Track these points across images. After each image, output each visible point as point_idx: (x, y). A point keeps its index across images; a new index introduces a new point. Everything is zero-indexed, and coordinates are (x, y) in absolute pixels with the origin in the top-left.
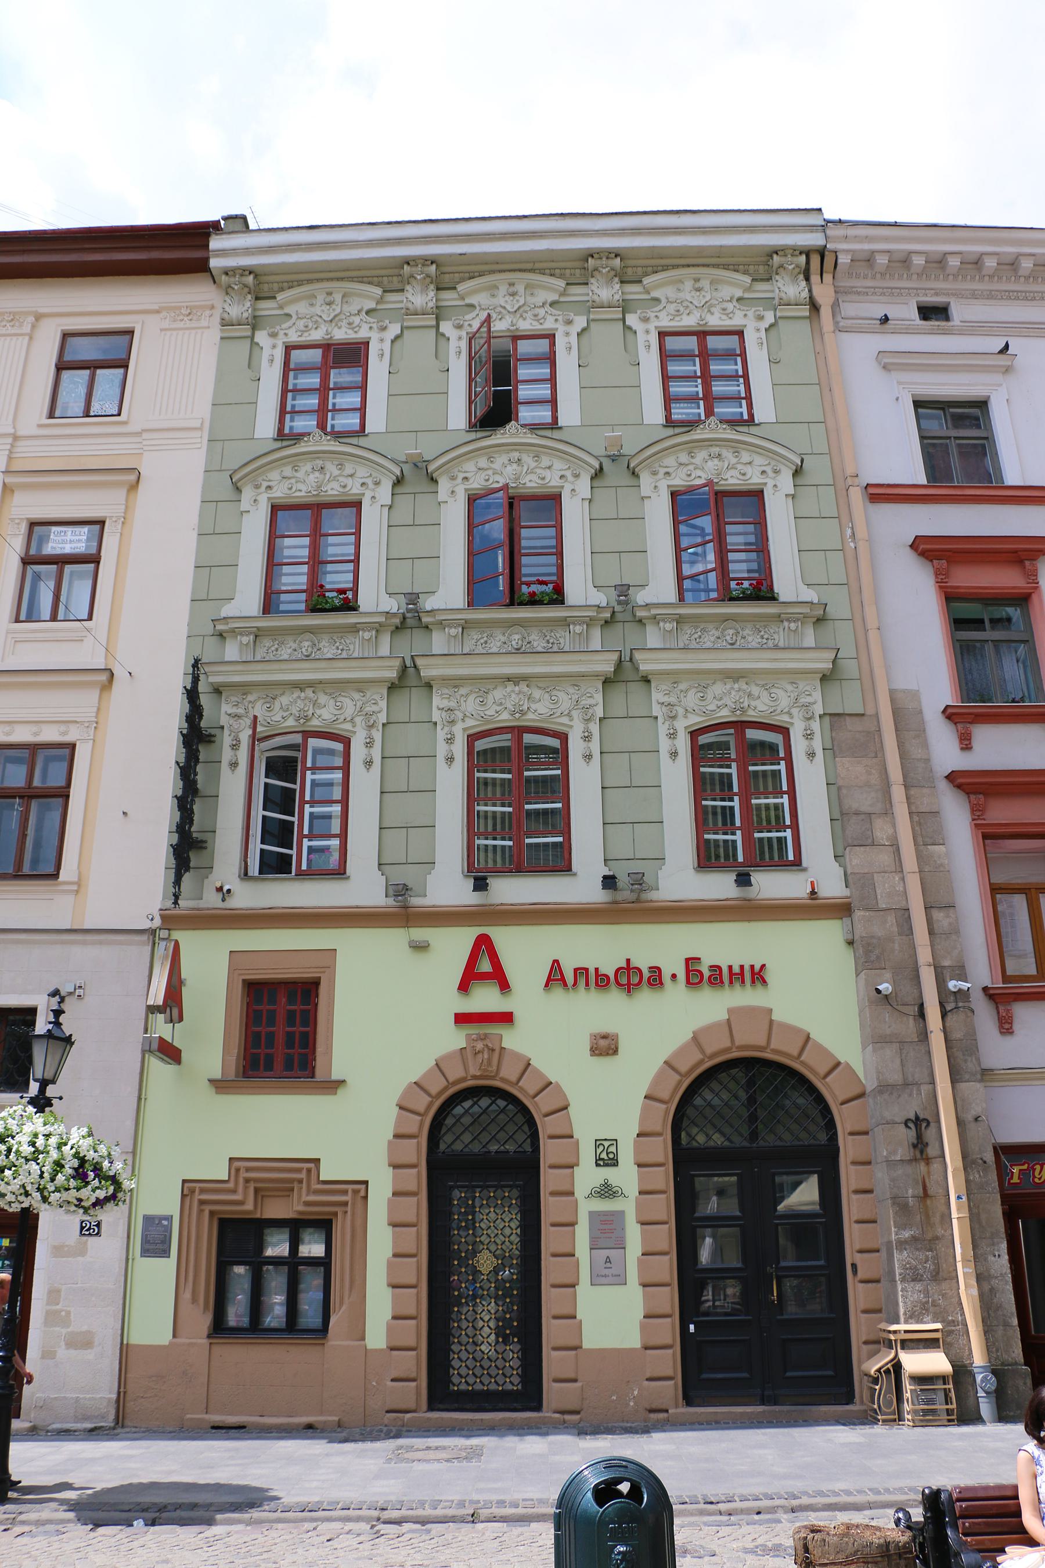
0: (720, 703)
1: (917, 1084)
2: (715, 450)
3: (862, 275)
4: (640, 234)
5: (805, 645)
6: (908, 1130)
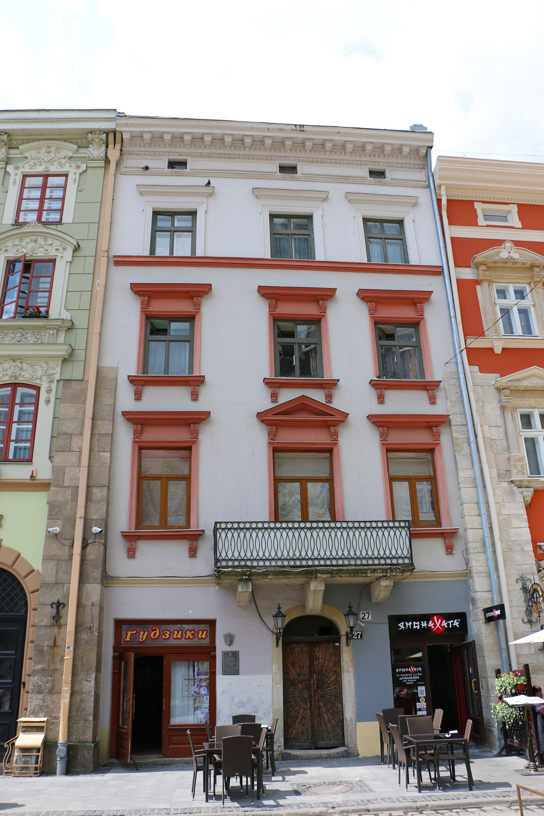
0: (5, 373)
1: (63, 584)
2: (34, 238)
3: (138, 144)
4: (17, 122)
5: (58, 342)
6: (52, 609)
